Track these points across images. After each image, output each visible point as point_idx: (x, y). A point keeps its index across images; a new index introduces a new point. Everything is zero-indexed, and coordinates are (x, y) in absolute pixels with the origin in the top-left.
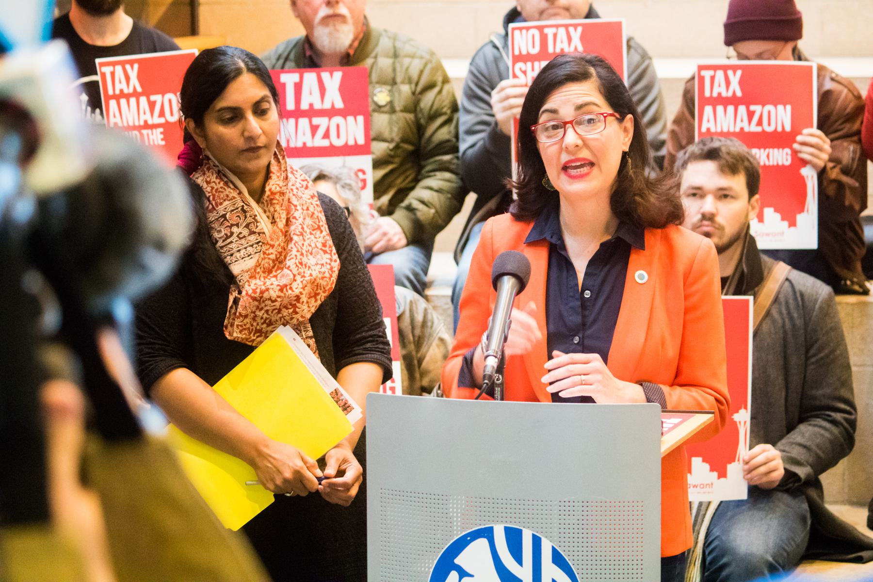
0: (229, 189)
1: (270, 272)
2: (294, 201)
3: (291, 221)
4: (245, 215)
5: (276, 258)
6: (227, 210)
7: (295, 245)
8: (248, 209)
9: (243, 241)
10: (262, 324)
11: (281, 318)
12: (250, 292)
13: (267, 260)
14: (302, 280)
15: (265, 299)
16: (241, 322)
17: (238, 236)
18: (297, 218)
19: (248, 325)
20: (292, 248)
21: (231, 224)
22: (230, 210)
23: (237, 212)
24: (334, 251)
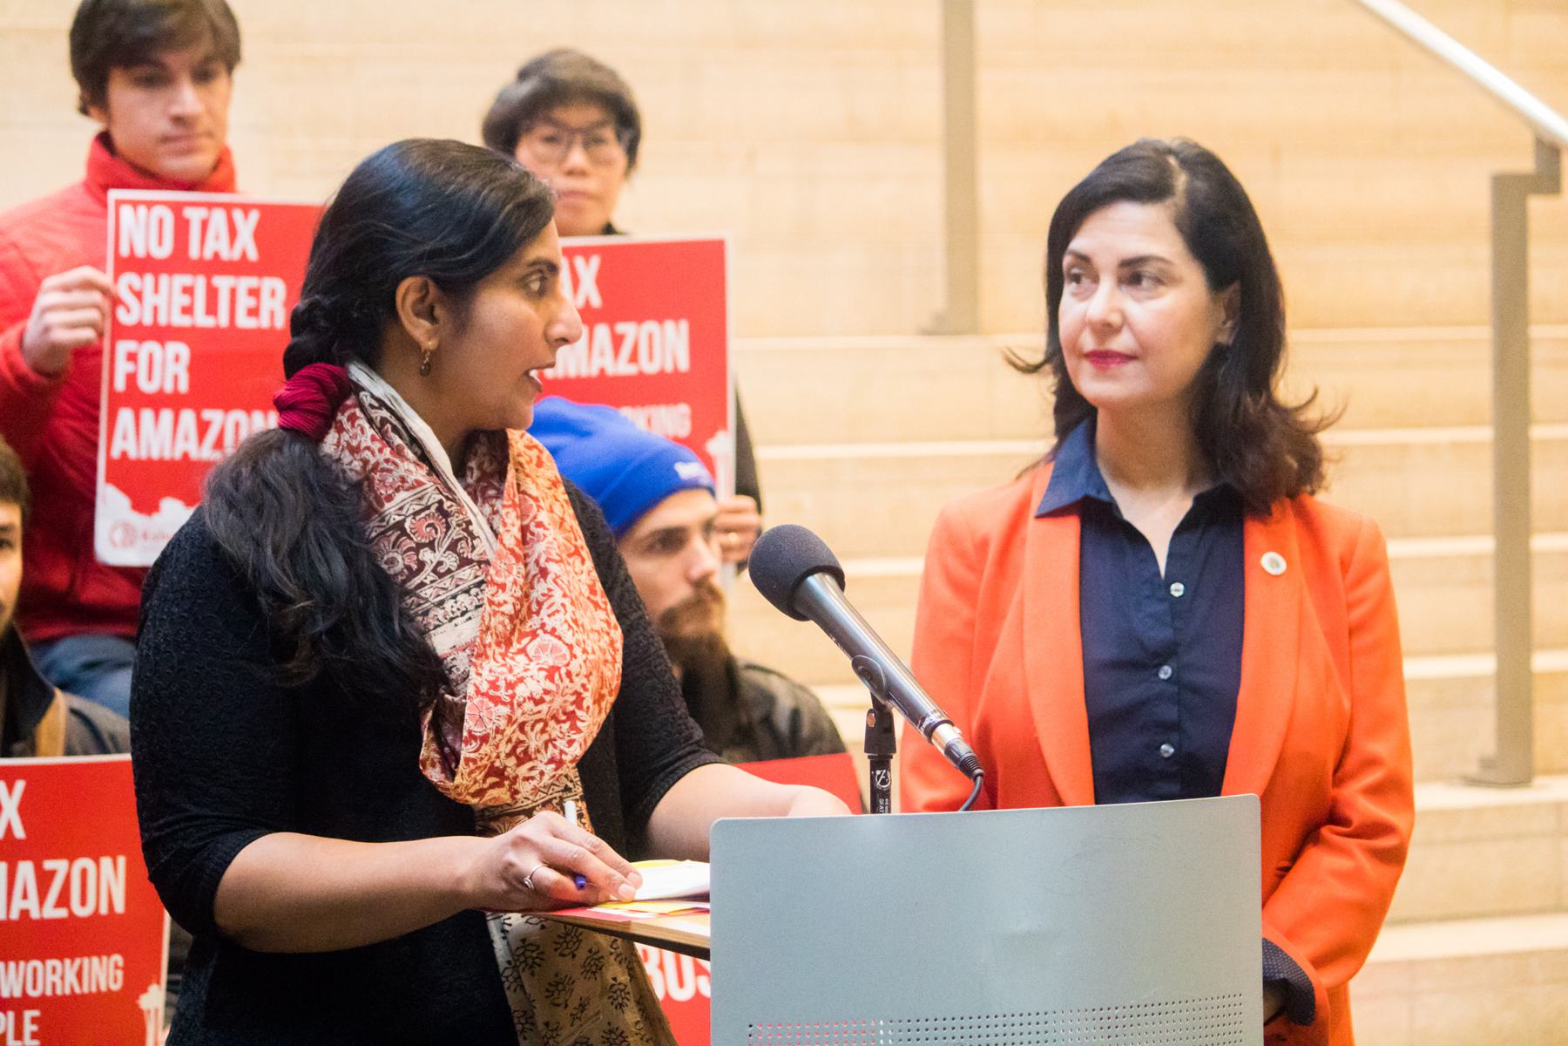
0: (406, 463)
1: (509, 643)
3: (532, 534)
4: (447, 522)
5: (515, 611)
6: (404, 512)
7: (555, 581)
8: (453, 509)
9: (447, 582)
10: (508, 755)
11: (546, 743)
12: (484, 687)
14: (584, 657)
15: (522, 699)
16: (475, 752)
17: (434, 571)
18: (547, 526)
20: (550, 590)
21: (417, 544)
22: (411, 511)
23: (429, 515)
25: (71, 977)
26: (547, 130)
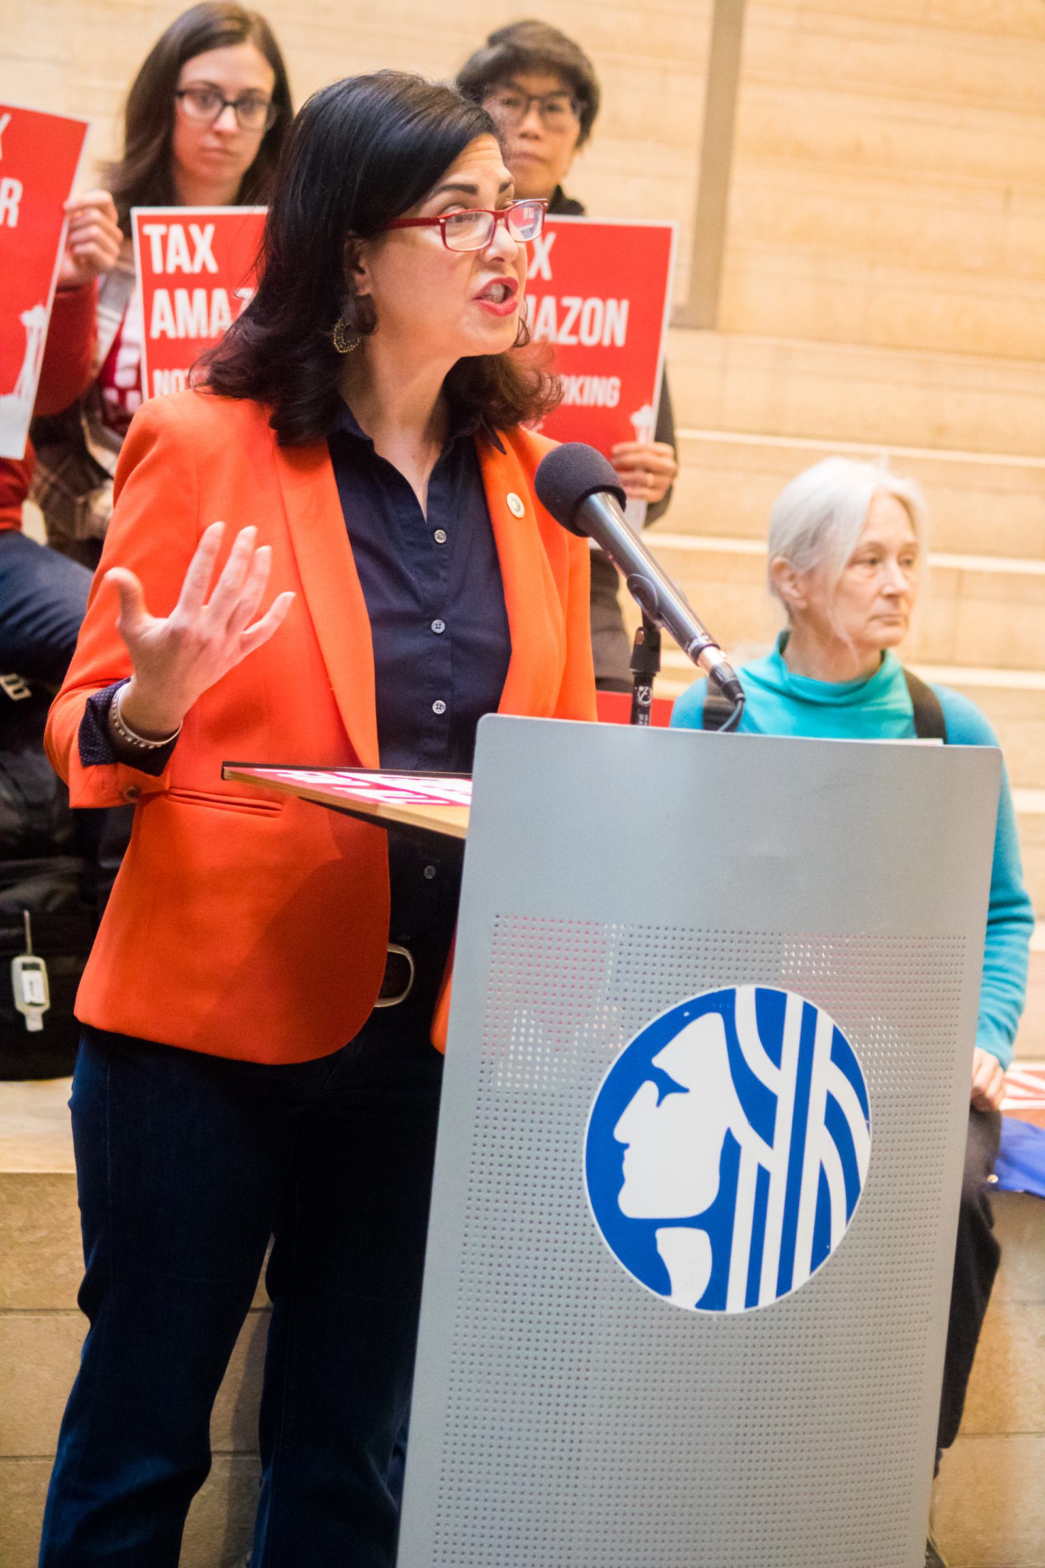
26: (507, 94)
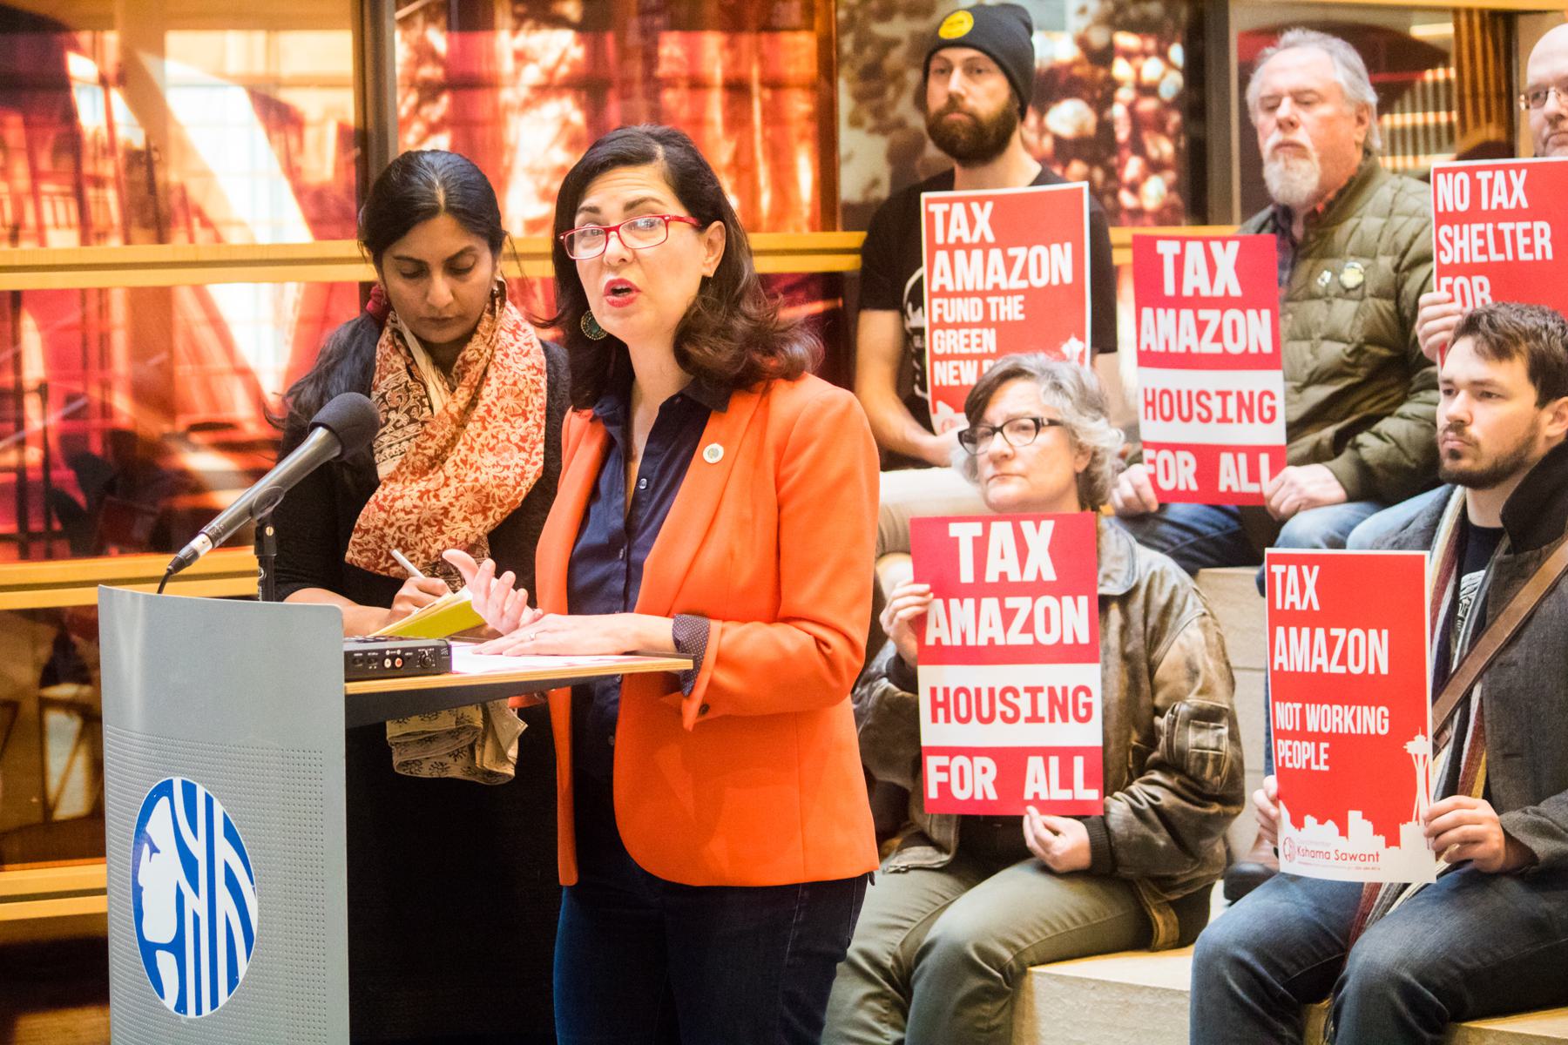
1: (426, 473)
2: (492, 373)
9: (399, 433)
11: (421, 540)
13: (420, 457)
17: (394, 426)
19: (374, 546)
24: (541, 447)
25: (1349, 720)
